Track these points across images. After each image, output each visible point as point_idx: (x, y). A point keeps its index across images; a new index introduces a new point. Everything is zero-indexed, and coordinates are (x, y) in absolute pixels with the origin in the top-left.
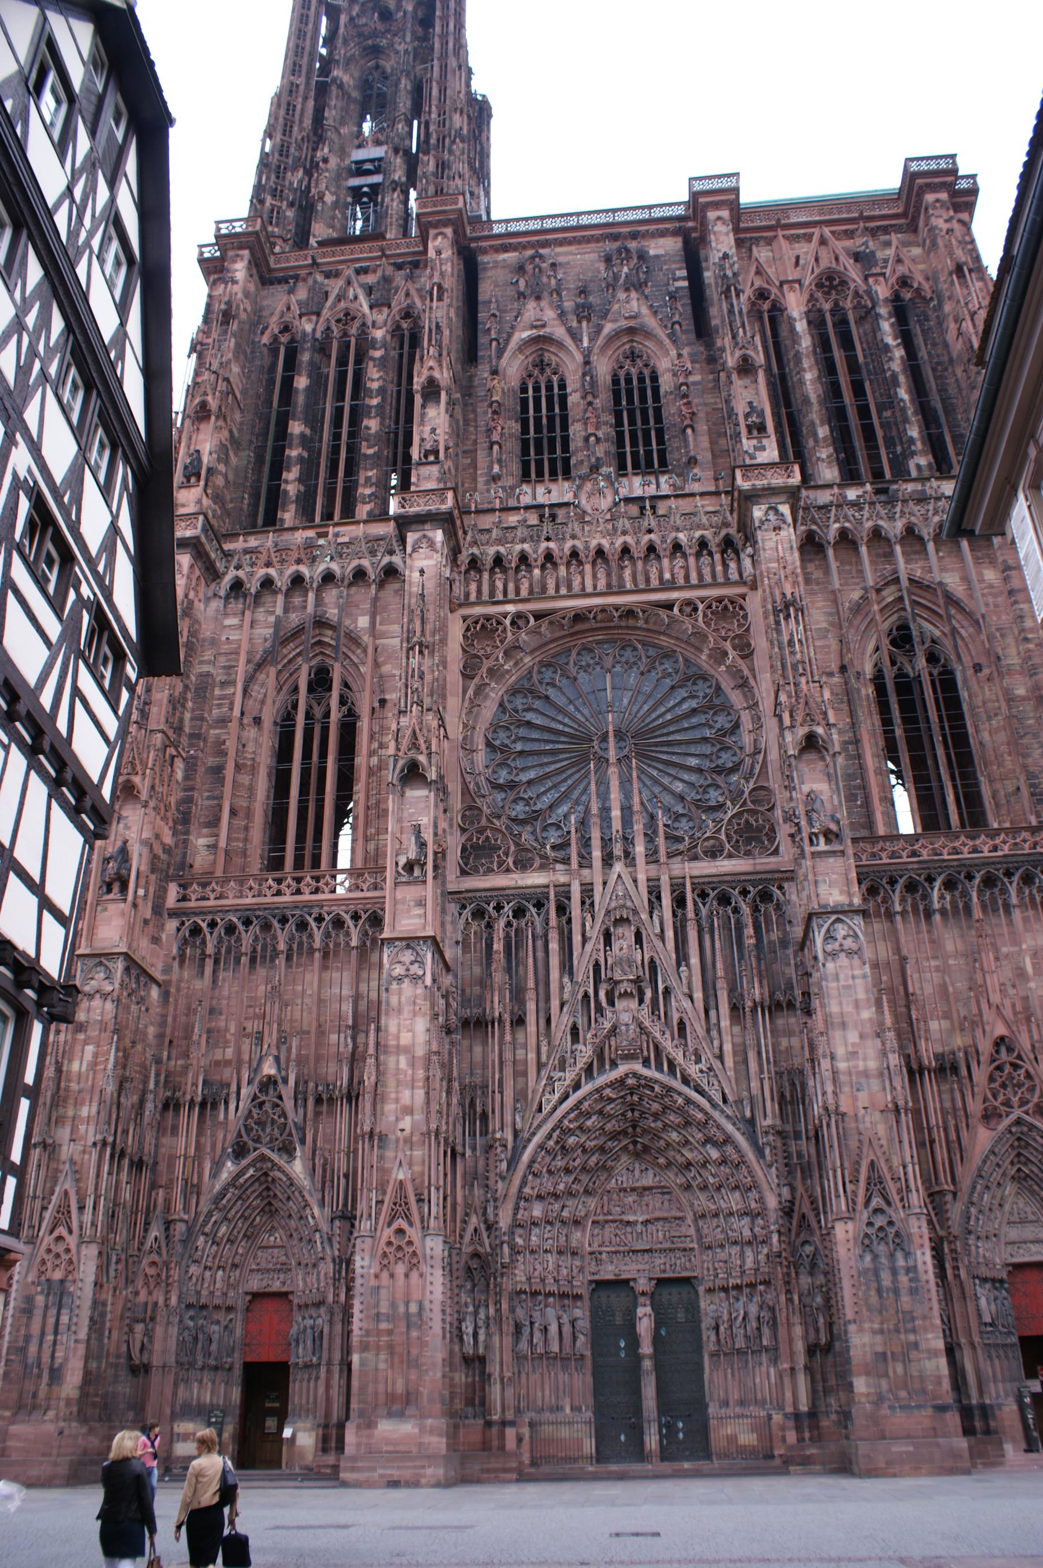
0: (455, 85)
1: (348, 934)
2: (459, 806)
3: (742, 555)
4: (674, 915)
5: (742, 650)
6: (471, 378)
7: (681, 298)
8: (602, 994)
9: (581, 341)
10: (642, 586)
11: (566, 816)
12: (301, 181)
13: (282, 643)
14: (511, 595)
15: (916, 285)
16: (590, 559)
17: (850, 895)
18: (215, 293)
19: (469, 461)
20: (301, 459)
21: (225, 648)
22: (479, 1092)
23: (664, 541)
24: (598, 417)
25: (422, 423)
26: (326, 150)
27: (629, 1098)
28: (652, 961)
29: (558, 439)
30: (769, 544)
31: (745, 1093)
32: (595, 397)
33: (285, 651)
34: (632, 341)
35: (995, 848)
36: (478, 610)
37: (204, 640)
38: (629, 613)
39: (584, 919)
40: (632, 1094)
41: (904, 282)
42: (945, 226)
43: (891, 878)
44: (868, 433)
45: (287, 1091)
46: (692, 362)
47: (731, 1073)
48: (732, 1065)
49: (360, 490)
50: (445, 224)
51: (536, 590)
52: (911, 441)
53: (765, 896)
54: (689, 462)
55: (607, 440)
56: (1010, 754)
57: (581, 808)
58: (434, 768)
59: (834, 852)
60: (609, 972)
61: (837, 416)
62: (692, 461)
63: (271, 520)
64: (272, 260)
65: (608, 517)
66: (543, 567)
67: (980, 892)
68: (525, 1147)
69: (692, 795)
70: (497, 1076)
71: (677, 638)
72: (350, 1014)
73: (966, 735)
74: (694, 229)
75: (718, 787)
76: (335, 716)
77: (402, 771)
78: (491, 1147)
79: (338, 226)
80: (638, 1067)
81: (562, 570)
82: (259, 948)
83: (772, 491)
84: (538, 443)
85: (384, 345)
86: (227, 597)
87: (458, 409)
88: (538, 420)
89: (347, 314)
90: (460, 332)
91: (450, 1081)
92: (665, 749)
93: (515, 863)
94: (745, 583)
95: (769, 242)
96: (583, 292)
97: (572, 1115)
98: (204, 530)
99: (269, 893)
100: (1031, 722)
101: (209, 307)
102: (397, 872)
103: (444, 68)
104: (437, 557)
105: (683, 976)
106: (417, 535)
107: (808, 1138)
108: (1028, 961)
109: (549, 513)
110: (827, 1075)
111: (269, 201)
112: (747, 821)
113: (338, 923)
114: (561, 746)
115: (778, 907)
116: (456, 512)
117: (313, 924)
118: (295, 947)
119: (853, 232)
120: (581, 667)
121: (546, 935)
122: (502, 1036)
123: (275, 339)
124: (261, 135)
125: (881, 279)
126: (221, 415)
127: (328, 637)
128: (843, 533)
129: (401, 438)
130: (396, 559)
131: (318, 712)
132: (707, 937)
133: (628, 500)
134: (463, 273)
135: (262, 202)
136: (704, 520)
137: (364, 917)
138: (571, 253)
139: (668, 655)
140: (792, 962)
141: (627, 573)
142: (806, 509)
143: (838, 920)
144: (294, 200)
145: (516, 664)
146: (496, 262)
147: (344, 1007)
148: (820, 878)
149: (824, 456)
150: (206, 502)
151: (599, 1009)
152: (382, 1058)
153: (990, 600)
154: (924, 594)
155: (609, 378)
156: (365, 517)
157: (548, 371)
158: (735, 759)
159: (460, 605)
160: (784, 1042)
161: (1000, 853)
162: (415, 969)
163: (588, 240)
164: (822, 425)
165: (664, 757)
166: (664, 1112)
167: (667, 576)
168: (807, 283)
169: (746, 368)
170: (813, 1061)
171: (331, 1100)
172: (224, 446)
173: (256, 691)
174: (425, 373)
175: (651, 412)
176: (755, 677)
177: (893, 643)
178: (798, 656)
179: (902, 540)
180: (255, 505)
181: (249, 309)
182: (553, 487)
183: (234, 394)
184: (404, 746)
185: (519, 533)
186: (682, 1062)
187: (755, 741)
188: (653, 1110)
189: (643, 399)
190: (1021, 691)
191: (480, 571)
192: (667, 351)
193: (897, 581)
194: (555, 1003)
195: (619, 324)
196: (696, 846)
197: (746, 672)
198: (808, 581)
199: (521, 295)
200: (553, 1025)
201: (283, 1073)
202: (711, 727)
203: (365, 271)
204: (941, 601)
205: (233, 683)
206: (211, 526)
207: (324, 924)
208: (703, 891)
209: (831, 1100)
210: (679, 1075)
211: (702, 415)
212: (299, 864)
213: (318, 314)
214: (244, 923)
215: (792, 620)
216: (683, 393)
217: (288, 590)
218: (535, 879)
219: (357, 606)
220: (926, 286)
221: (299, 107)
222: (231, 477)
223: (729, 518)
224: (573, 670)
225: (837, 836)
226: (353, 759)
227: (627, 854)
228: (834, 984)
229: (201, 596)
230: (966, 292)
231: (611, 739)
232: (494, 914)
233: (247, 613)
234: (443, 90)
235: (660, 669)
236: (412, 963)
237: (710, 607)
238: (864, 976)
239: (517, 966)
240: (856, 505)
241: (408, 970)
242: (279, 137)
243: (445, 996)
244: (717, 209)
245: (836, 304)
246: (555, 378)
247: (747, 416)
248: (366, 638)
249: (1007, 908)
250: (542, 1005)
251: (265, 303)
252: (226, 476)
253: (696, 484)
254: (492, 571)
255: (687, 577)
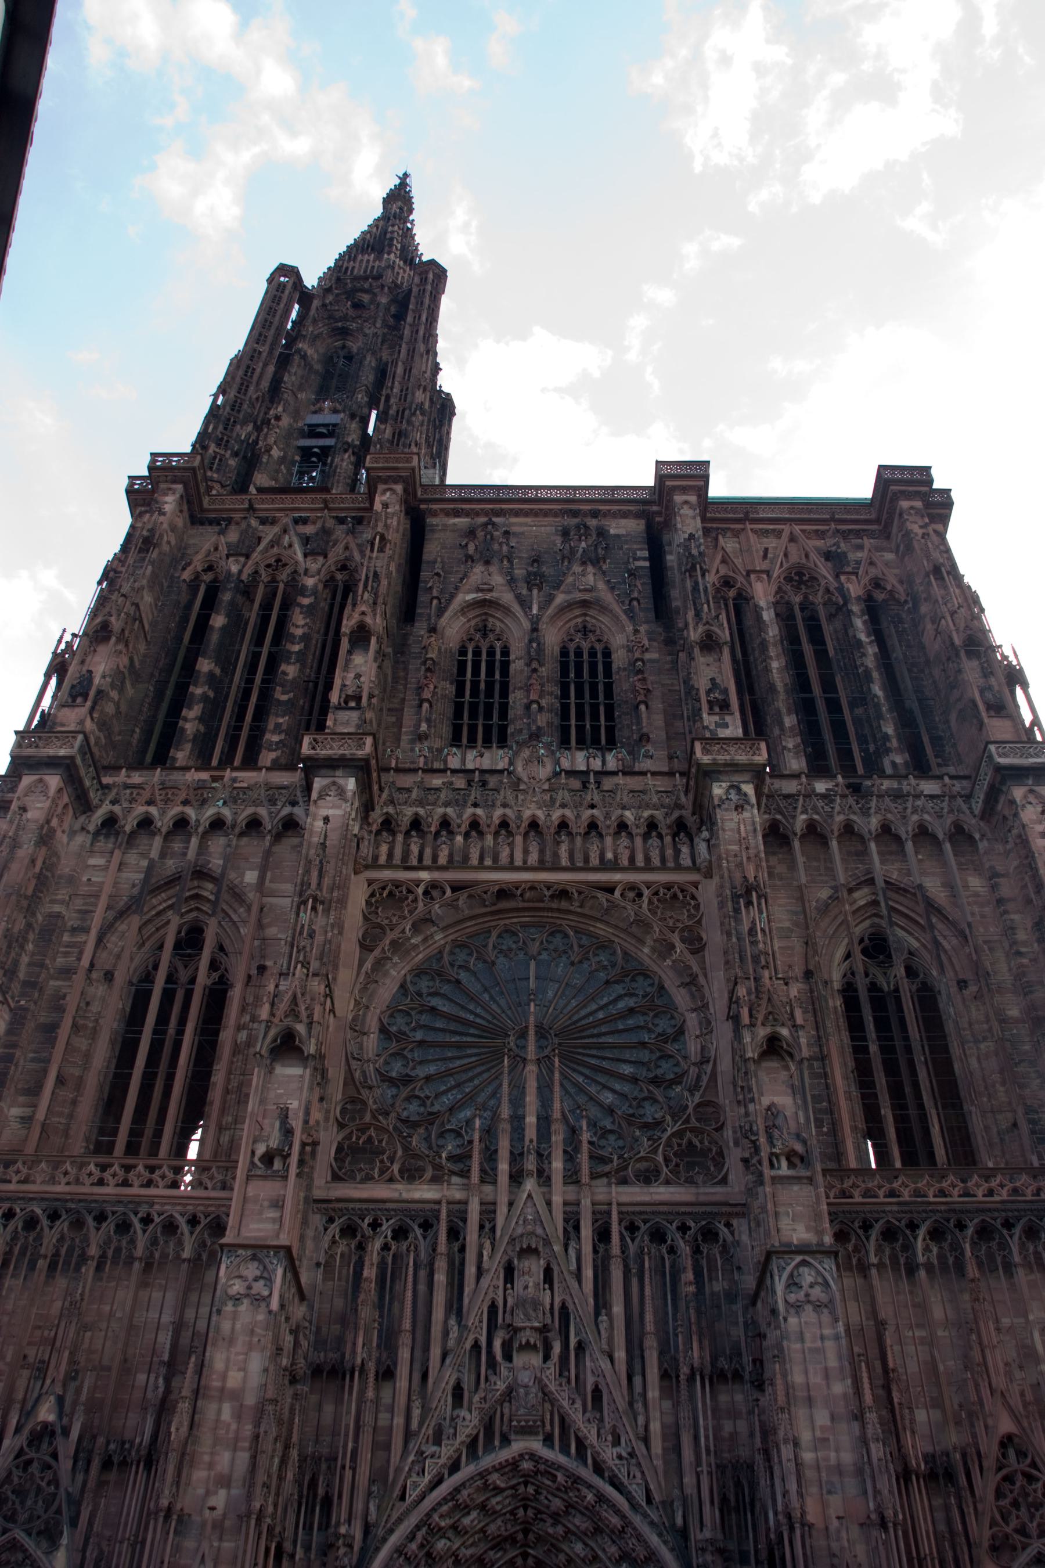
0: (420, 366)
1: (180, 1243)
2: (340, 1096)
3: (696, 840)
4: (595, 1251)
5: (691, 943)
6: (405, 637)
7: (640, 577)
8: (497, 1344)
9: (530, 608)
10: (580, 864)
11: (469, 1122)
12: (249, 435)
13: (152, 891)
14: (427, 861)
15: (889, 588)
16: (522, 830)
17: (820, 1233)
18: (139, 525)
19: (394, 719)
20: (205, 698)
21: (84, 890)
22: (324, 1466)
23: (607, 816)
24: (542, 685)
25: (346, 668)
26: (280, 409)
27: (521, 1489)
28: (564, 1307)
29: (496, 706)
30: (729, 825)
31: (676, 1492)
32: (541, 665)
33: (154, 901)
34: (585, 615)
35: (991, 1193)
36: (387, 874)
37: (60, 877)
38: (563, 894)
39: (481, 1247)
40: (526, 1484)
41: (877, 584)
42: (920, 532)
43: (864, 1221)
44: (839, 728)
45: (66, 1448)
46: (650, 640)
47: (658, 1463)
48: (659, 1451)
49: (268, 736)
50: (396, 480)
51: (457, 858)
52: (886, 737)
53: (709, 1234)
54: (641, 740)
55: (550, 711)
56: (1003, 1084)
57: (487, 1114)
58: (313, 1041)
59: (799, 1178)
60: (507, 1315)
61: (806, 708)
62: (644, 738)
63: (162, 759)
64: (206, 501)
65: (546, 787)
66: (467, 835)
67: (973, 1244)
68: (378, 1549)
69: (623, 1109)
70: (350, 1445)
71: (616, 927)
72: (168, 1346)
73: (949, 1063)
74: (659, 513)
75: (656, 1101)
76: (203, 978)
77: (275, 1040)
78: (331, 1546)
79: (281, 479)
80: (536, 1445)
81: (489, 840)
82: (63, 1251)
83: (734, 768)
84: (474, 708)
85: (315, 592)
86: (97, 834)
87: (388, 664)
88: (475, 685)
89: (278, 561)
90: (399, 588)
91: (287, 1447)
92: (594, 1052)
93: (400, 1171)
94: (698, 870)
95: (736, 534)
96: (536, 561)
97: (445, 1508)
98: (82, 751)
99: (88, 1181)
100: (1027, 1047)
101: (129, 537)
102: (252, 1163)
103: (412, 352)
104: (347, 806)
105: (603, 1327)
106: (326, 781)
107: (757, 1562)
108: (1037, 1335)
109: (478, 779)
110: (792, 1465)
111: (213, 448)
112: (690, 1142)
113: (170, 1227)
114: (469, 1039)
115: (725, 1249)
116: (373, 762)
117: (138, 1225)
118: (110, 1253)
119: (823, 532)
120: (501, 951)
121: (431, 1265)
122: (362, 1392)
123: (197, 577)
124: (214, 390)
125: (854, 577)
126: (122, 638)
127: (208, 890)
128: (811, 828)
129: (320, 688)
130: (298, 811)
131: (183, 976)
132: (635, 1282)
133: (572, 773)
134: (408, 533)
135: (205, 448)
136: (655, 799)
137: (204, 1222)
138: (526, 525)
139: (604, 945)
140: (741, 1319)
141: (563, 850)
142: (770, 796)
143: (804, 1263)
144: (239, 450)
145: (425, 940)
146: (445, 525)
147: (161, 1338)
148: (781, 1209)
149: (790, 746)
150: (89, 725)
151: (492, 1364)
152: (199, 1403)
153: (976, 909)
154: (901, 899)
155: (557, 650)
156: (268, 764)
157: (491, 636)
158: (676, 1069)
159: (367, 867)
160: (728, 1427)
161: (996, 1198)
162: (259, 1287)
163: (546, 514)
164: (789, 714)
165: (593, 1061)
166: (567, 1513)
167: (609, 855)
168: (775, 575)
169: (709, 644)
170: (766, 1452)
171: (124, 1464)
172: (122, 673)
173: (113, 941)
174: (356, 617)
175: (601, 687)
176: (706, 976)
177: (864, 952)
178: (761, 946)
179: (877, 838)
180: (145, 742)
181: (173, 543)
182: (487, 754)
183: (141, 622)
184: (280, 1012)
185: (443, 796)
186: (595, 1442)
187: (703, 1048)
188: (553, 1508)
189: (593, 673)
190: (1014, 1012)
191: (393, 833)
192: (623, 627)
193: (873, 879)
194: (435, 1352)
195: (572, 596)
196: (626, 1168)
197: (696, 969)
198: (771, 875)
199: (469, 558)
200: (431, 1381)
201: (65, 1420)
202: (650, 1031)
203: (304, 521)
204: (921, 908)
205: (86, 930)
206: (91, 754)
207: (151, 1227)
208: (632, 1223)
209: (795, 1503)
210: (590, 1461)
211: (657, 693)
212: (132, 1149)
213: (247, 556)
214: (49, 1217)
215: (754, 911)
216: (636, 668)
217: (168, 833)
218: (424, 1192)
219: (247, 859)
220: (900, 589)
221: (258, 370)
222: (123, 708)
223: (683, 799)
224: (491, 954)
225: (802, 1159)
226: (217, 1033)
227: (540, 1172)
228: (798, 1346)
229: (66, 826)
230: (943, 592)
231: (532, 1032)
232: (369, 1232)
233: (117, 851)
234: (408, 371)
235: (594, 960)
236: (256, 1279)
237: (656, 893)
238: (837, 1337)
239: (391, 1303)
240: (825, 797)
241: (249, 1288)
242: (232, 393)
243: (295, 1332)
244: (684, 493)
245: (806, 597)
246: (498, 645)
247: (709, 692)
248: (251, 896)
249: (1008, 1267)
250: (418, 1354)
251: (192, 541)
252: (117, 705)
253: (649, 761)
254: (407, 834)
255: (632, 859)
